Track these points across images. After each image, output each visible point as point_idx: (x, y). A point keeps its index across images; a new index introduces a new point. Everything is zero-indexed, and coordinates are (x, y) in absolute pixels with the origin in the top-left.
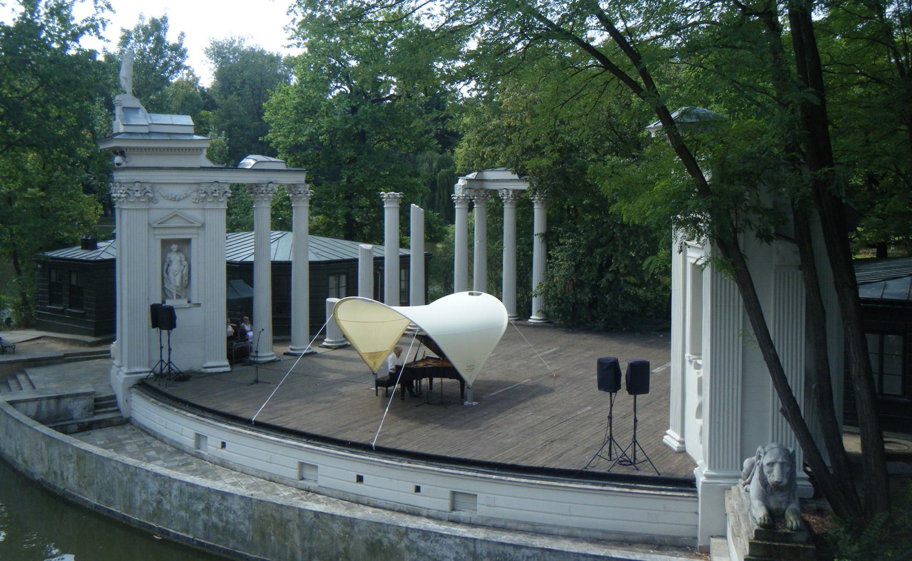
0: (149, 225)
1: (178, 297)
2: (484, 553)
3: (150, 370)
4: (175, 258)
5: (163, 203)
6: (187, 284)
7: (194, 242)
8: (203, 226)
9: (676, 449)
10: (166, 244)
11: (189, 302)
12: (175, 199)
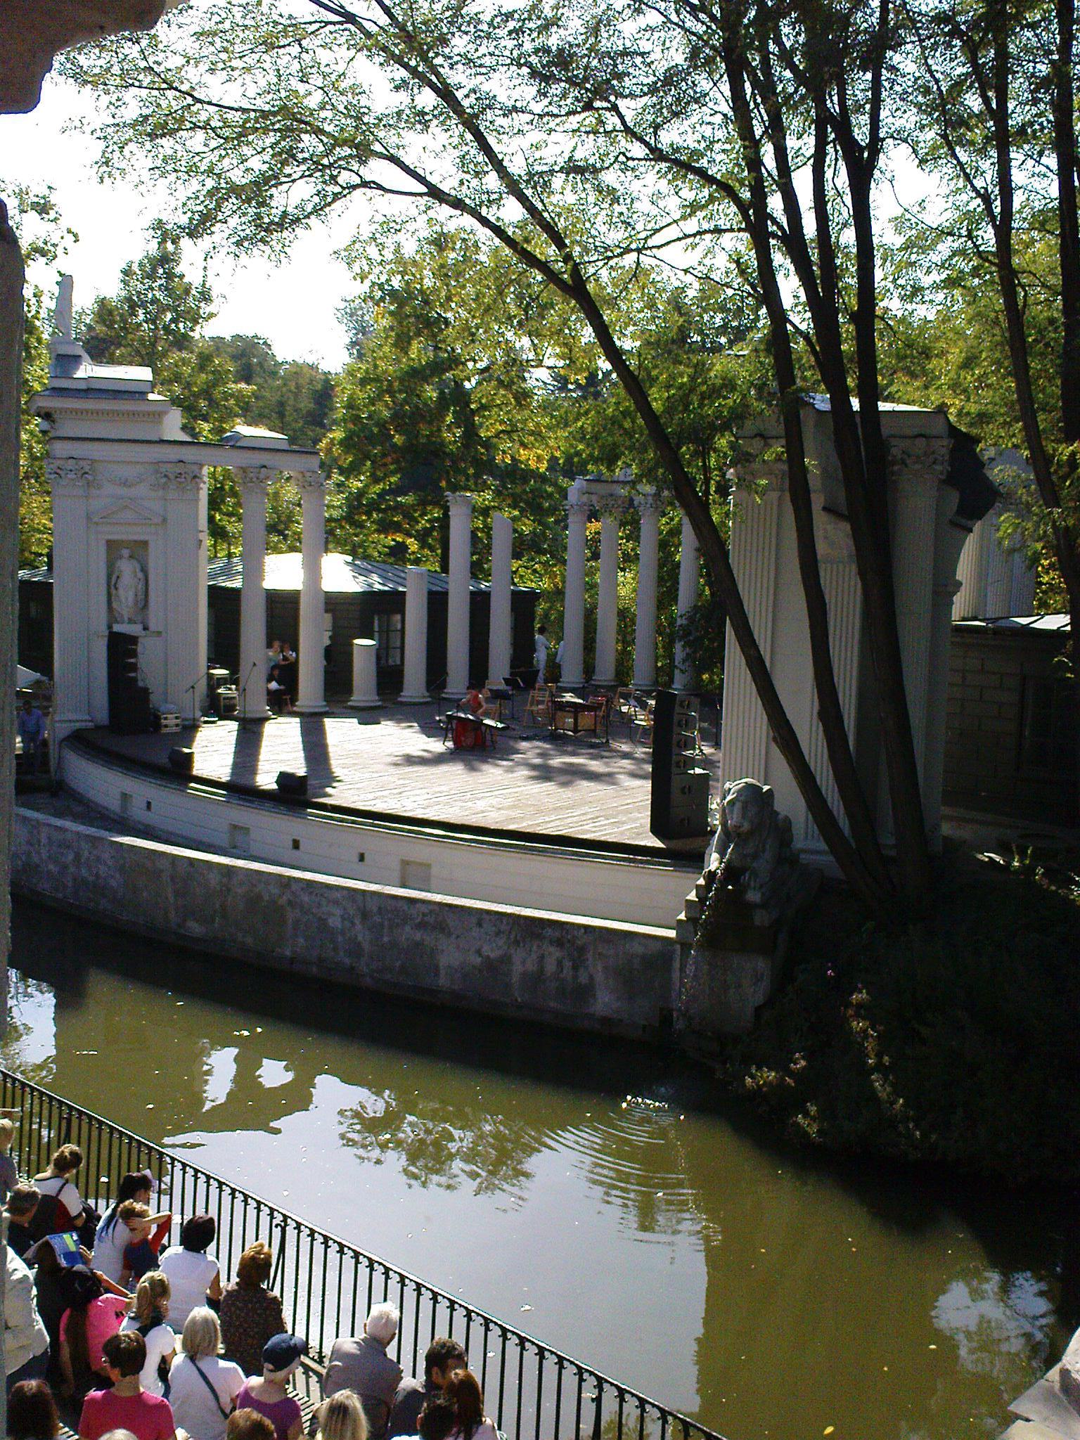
0: (89, 518)
1: (131, 621)
2: (375, 909)
3: (87, 717)
4: (127, 569)
6: (143, 604)
7: (151, 544)
8: (165, 520)
10: (113, 547)
11: (145, 629)
12: (125, 483)
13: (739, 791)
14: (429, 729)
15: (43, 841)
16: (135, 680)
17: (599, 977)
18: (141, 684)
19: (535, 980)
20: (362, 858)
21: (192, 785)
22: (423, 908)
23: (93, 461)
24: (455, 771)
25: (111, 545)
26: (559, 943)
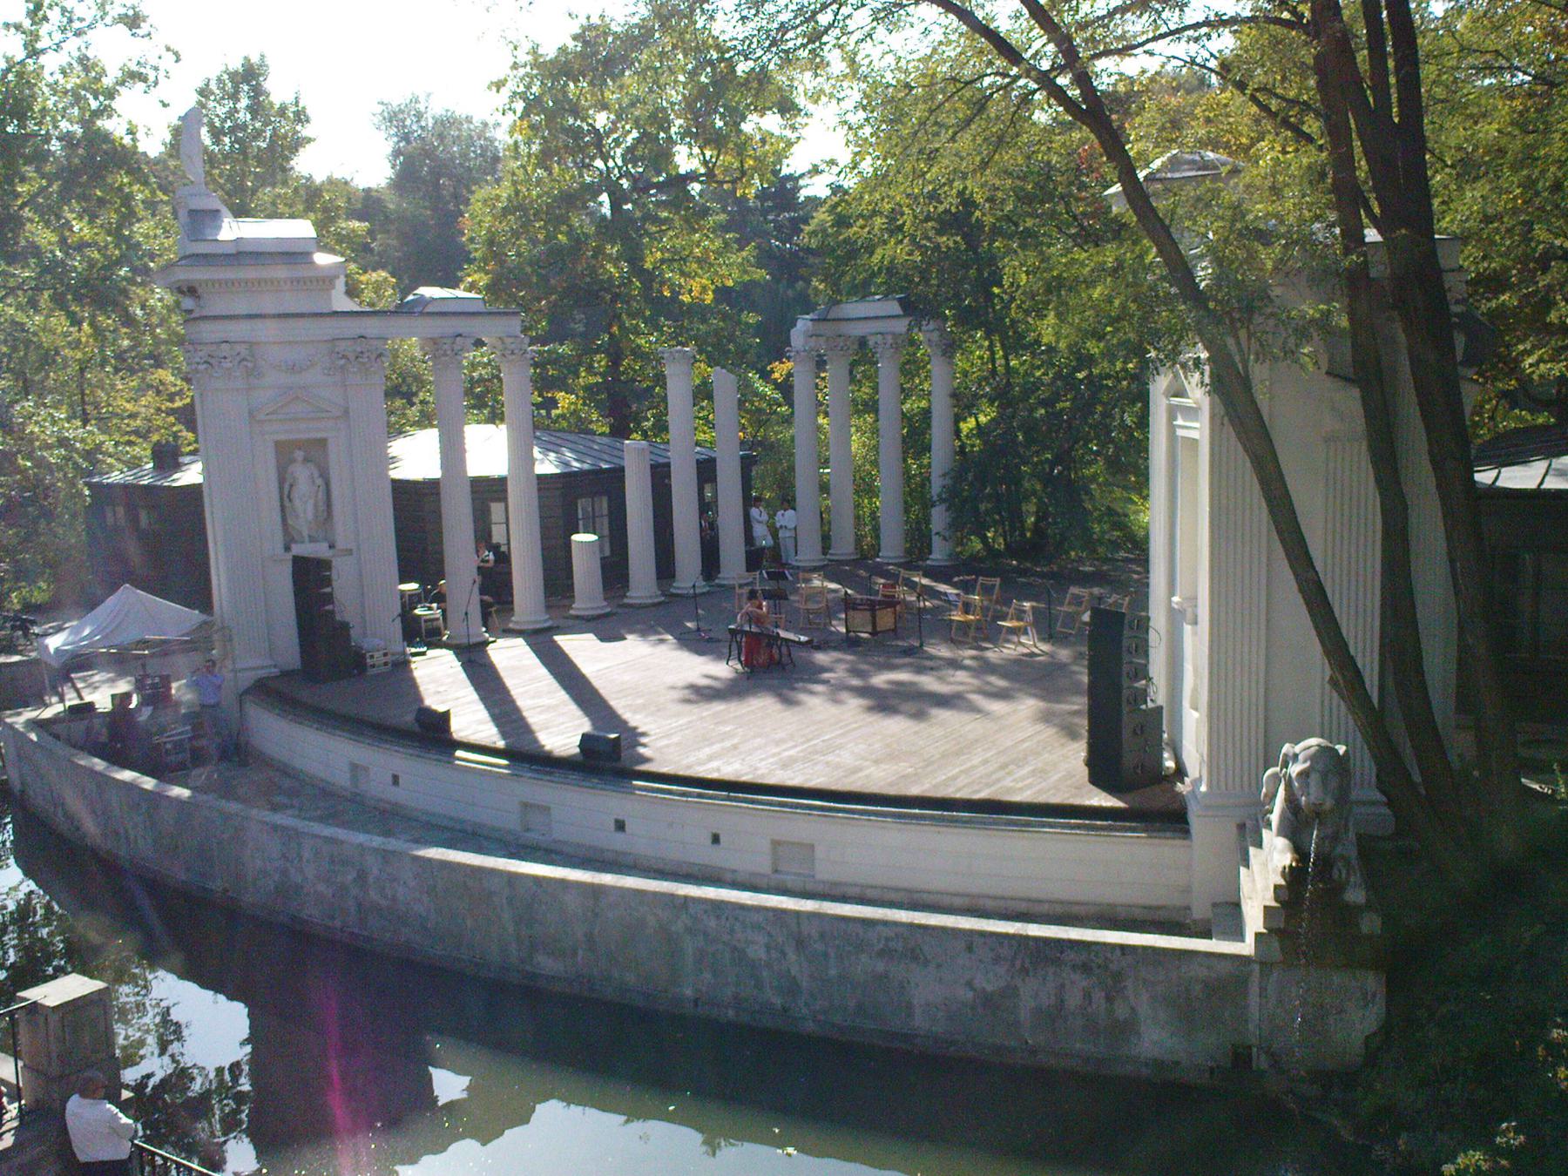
0: (251, 414)
1: (312, 539)
4: (302, 475)
8: (346, 412)
11: (331, 547)
13: (1313, 758)
14: (697, 643)
15: (306, 855)
16: (332, 612)
17: (1144, 1010)
18: (338, 618)
19: (1053, 1015)
20: (716, 839)
21: (459, 753)
22: (886, 932)
23: (251, 344)
24: (762, 706)
25: (278, 444)
26: (1086, 968)
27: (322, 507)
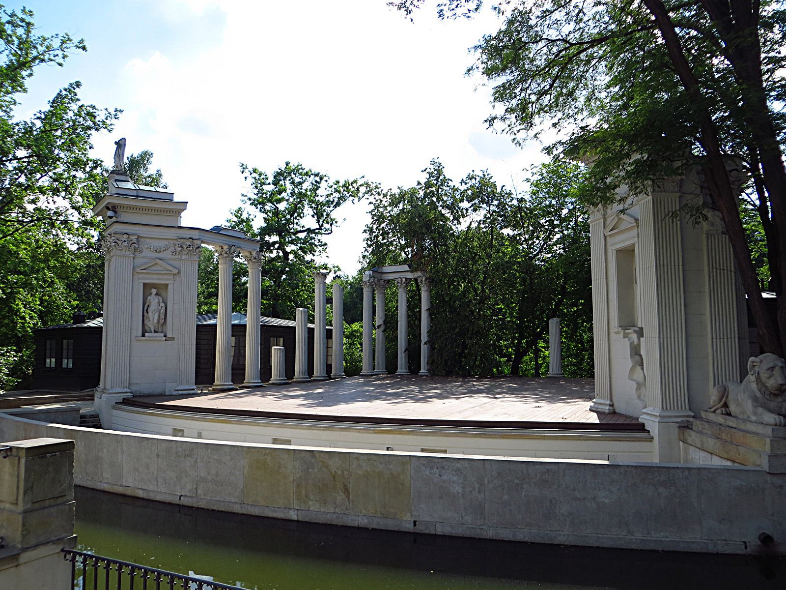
1: (155, 332)
4: (154, 300)
5: (147, 253)
7: (170, 287)
9: (607, 411)
11: (165, 336)
27: (162, 316)
